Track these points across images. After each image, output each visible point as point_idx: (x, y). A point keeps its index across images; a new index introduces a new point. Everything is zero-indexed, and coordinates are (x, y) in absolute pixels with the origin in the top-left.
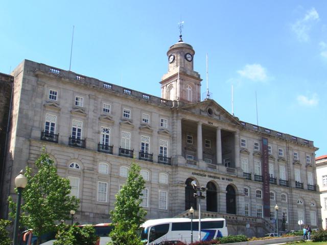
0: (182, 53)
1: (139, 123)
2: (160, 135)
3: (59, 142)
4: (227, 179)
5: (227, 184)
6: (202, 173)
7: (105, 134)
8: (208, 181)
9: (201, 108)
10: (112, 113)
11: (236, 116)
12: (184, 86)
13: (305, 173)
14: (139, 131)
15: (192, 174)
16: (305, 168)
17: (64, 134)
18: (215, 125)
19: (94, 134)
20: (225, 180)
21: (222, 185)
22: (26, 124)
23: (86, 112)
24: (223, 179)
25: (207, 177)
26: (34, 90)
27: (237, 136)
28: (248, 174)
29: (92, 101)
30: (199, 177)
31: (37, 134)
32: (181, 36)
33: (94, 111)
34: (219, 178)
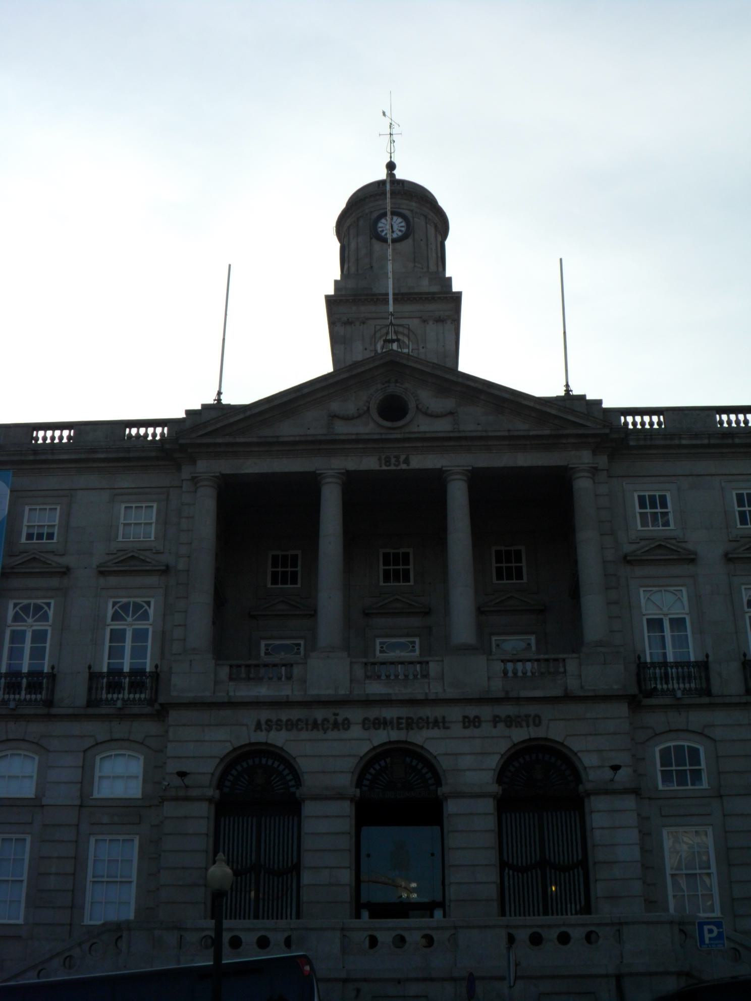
0: (361, 222)
2: (112, 580)
4: (496, 720)
5: (503, 747)
6: (320, 714)
8: (364, 748)
9: (335, 406)
11: (576, 391)
15: (258, 727)
24: (470, 722)
25: (356, 731)
27: (582, 484)
28: (697, 664)
30: (304, 735)
32: (391, 166)
34: (440, 723)
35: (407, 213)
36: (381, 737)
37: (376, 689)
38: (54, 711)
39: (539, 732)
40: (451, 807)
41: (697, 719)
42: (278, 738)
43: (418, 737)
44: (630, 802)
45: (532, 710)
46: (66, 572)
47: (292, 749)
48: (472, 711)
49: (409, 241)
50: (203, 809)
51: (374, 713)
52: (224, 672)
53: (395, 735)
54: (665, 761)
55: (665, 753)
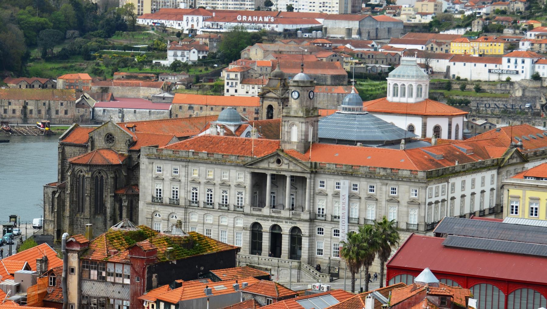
1: (219, 179)
3: (164, 202)
4: (290, 222)
5: (291, 227)
6: (265, 218)
7: (195, 191)
8: (271, 225)
10: (199, 175)
12: (286, 127)
13: (405, 209)
14: (219, 186)
16: (406, 204)
17: (167, 196)
18: (282, 173)
19: (186, 194)
20: (288, 223)
21: (286, 228)
22: (144, 192)
23: (180, 178)
24: (286, 222)
25: (270, 222)
26: (147, 168)
27: (308, 180)
29: (184, 169)
31: (149, 199)
33: (185, 176)
34: (282, 222)
35: (299, 91)
36: (274, 223)
37: (273, 214)
38: (229, 211)
39: (296, 225)
40: (283, 236)
41: (323, 224)
42: (259, 221)
43: (279, 224)
44: (308, 238)
45: (295, 222)
46: (230, 186)
47: (261, 224)
48: (287, 221)
49: (299, 99)
50: (249, 232)
51: (273, 219)
52: (252, 209)
53: (276, 223)
54: (318, 230)
55: (318, 228)
